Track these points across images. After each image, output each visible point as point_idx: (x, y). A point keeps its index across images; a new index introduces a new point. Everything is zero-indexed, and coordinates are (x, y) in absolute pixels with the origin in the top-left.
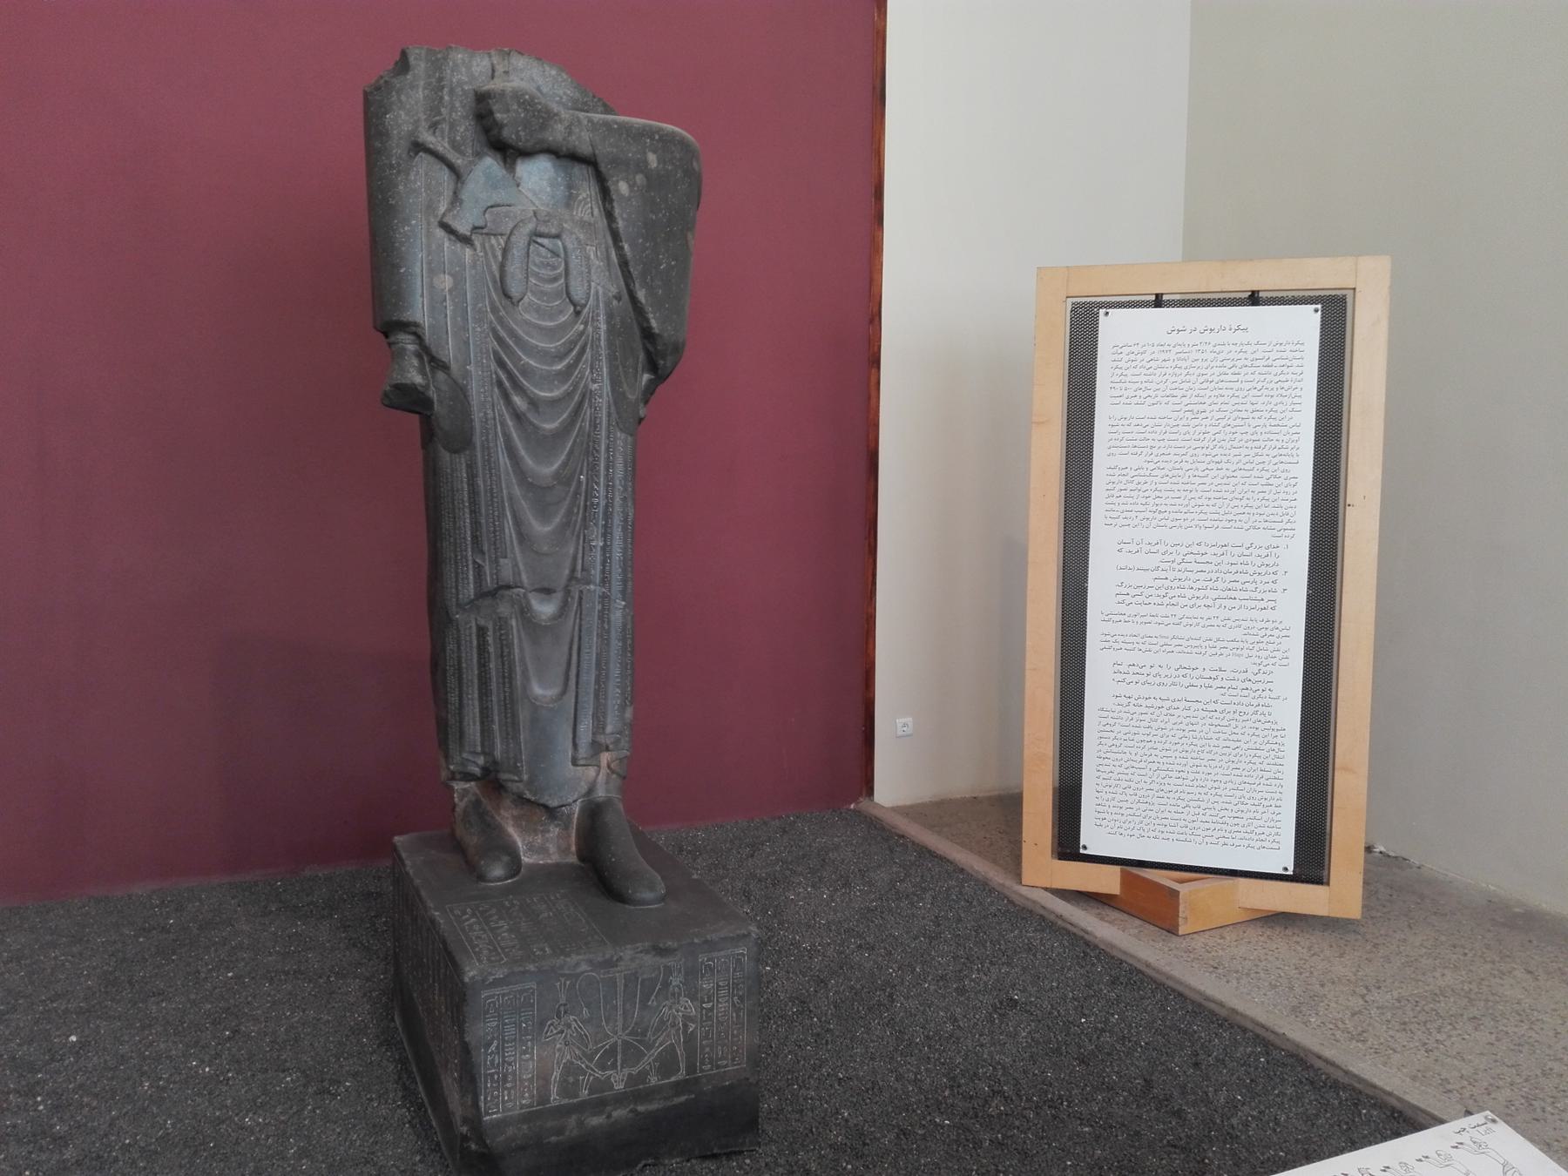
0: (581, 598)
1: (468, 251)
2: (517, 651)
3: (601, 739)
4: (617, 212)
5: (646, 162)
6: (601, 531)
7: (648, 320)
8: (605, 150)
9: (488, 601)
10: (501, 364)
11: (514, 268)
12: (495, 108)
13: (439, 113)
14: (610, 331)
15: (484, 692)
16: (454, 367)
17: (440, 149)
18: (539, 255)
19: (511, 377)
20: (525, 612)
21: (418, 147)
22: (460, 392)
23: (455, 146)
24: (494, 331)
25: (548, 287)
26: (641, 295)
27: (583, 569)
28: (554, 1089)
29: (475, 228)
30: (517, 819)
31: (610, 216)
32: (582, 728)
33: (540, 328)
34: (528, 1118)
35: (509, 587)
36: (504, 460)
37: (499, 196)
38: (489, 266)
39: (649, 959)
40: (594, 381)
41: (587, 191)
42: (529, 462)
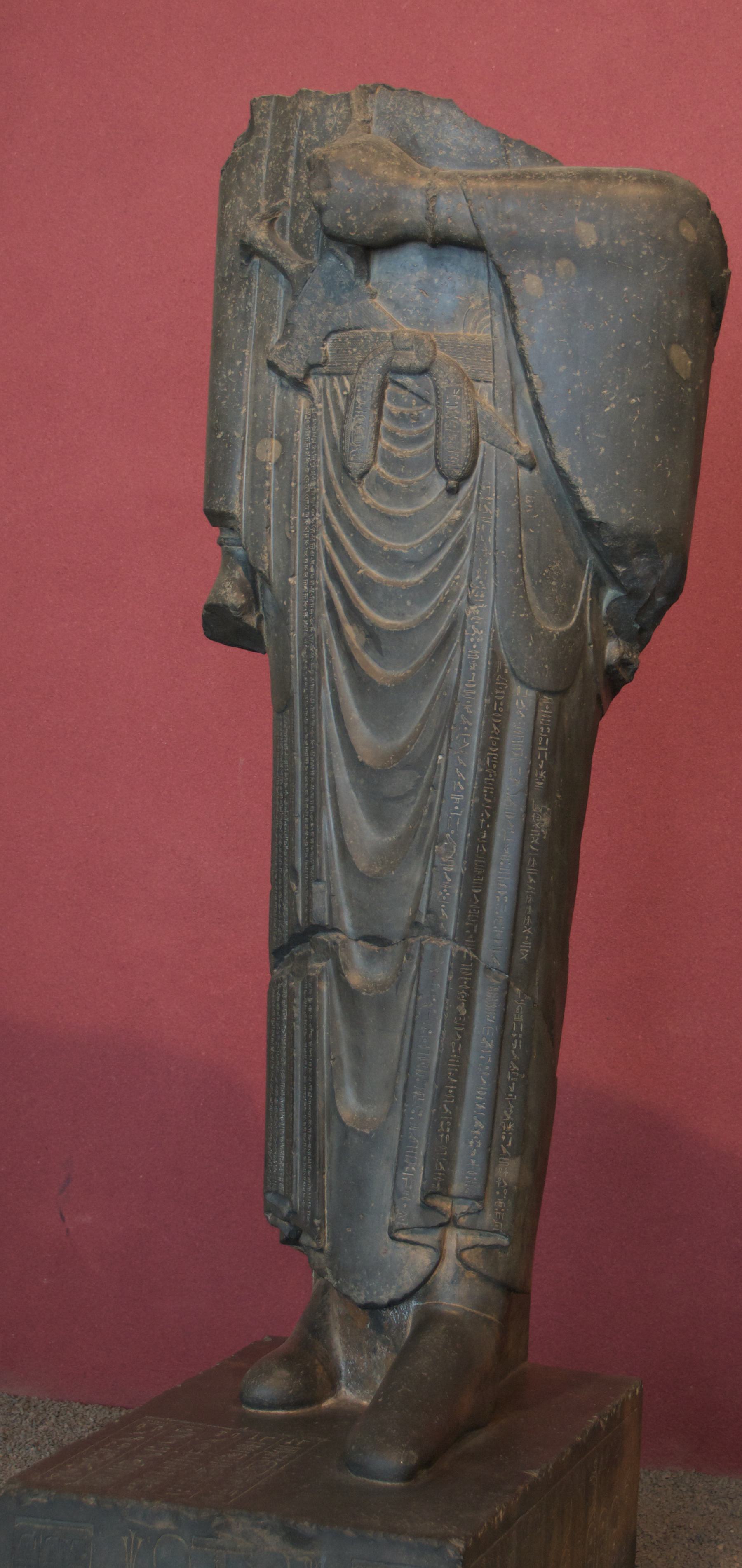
0: (420, 959)
1: (303, 402)
3: (445, 1205)
11: (361, 427)
13: (282, 196)
16: (274, 577)
18: (398, 401)
23: (298, 245)
24: (327, 521)
25: (407, 452)
26: (564, 456)
27: (429, 912)
32: (405, 1175)
33: (389, 518)
37: (346, 314)
38: (329, 423)
39: (273, 1543)
42: (362, 733)
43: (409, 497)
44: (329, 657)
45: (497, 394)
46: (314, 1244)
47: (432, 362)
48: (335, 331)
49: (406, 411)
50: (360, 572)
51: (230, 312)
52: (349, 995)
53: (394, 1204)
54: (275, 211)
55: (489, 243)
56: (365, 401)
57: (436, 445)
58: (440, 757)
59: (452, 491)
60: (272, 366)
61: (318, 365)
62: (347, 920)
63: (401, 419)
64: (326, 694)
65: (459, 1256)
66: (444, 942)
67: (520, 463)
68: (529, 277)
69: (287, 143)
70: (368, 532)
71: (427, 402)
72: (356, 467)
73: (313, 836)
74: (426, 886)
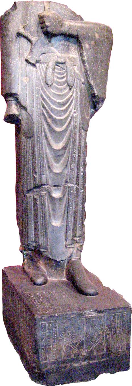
1: (34, 69)
2: (47, 207)
3: (75, 239)
4: (84, 54)
5: (95, 37)
6: (76, 165)
7: (93, 91)
8: (81, 34)
9: (38, 190)
10: (44, 107)
11: (49, 74)
12: (46, 21)
14: (80, 95)
15: (36, 222)
17: (26, 35)
18: (58, 69)
19: (47, 112)
20: (49, 194)
21: (19, 35)
22: (30, 116)
24: (42, 96)
26: (92, 82)
28: (63, 354)
29: (37, 61)
30: (46, 265)
31: (81, 55)
32: (68, 234)
33: (58, 95)
34: (54, 363)
35: (45, 185)
36: (44, 142)
40: (75, 113)
41: (74, 47)
42: (52, 142)
43: (61, 90)
44: (44, 125)
45: (78, 68)
46: (46, 251)
47: (66, 61)
48: (43, 54)
49: (60, 72)
50: (51, 107)
51: (13, 48)
52: (52, 199)
53: (66, 240)
54: (25, 26)
55: (79, 36)
56: (50, 69)
57: (67, 79)
58: (70, 146)
59: (70, 89)
60: (27, 61)
61: (39, 61)
62: (50, 182)
63: (59, 73)
64: (43, 133)
65: (77, 248)
66: (73, 185)
67: (83, 83)
68: (86, 44)
69: (27, 11)
70: (53, 98)
71: (64, 70)
72: (50, 83)
73: (41, 166)
74: (69, 174)
